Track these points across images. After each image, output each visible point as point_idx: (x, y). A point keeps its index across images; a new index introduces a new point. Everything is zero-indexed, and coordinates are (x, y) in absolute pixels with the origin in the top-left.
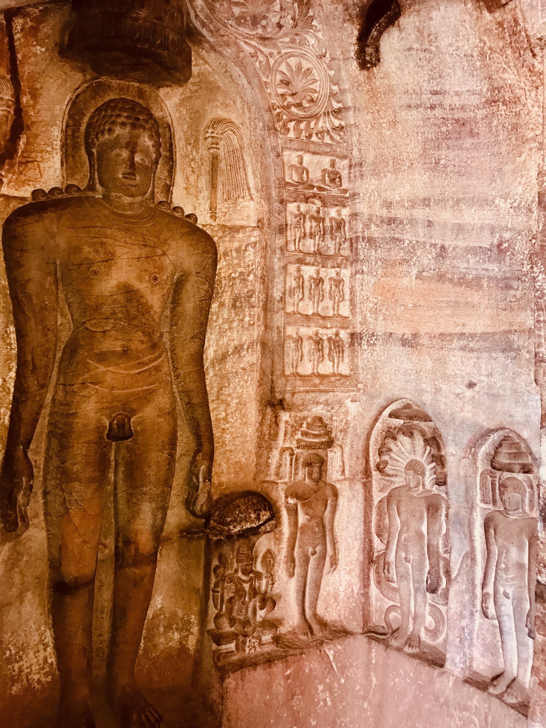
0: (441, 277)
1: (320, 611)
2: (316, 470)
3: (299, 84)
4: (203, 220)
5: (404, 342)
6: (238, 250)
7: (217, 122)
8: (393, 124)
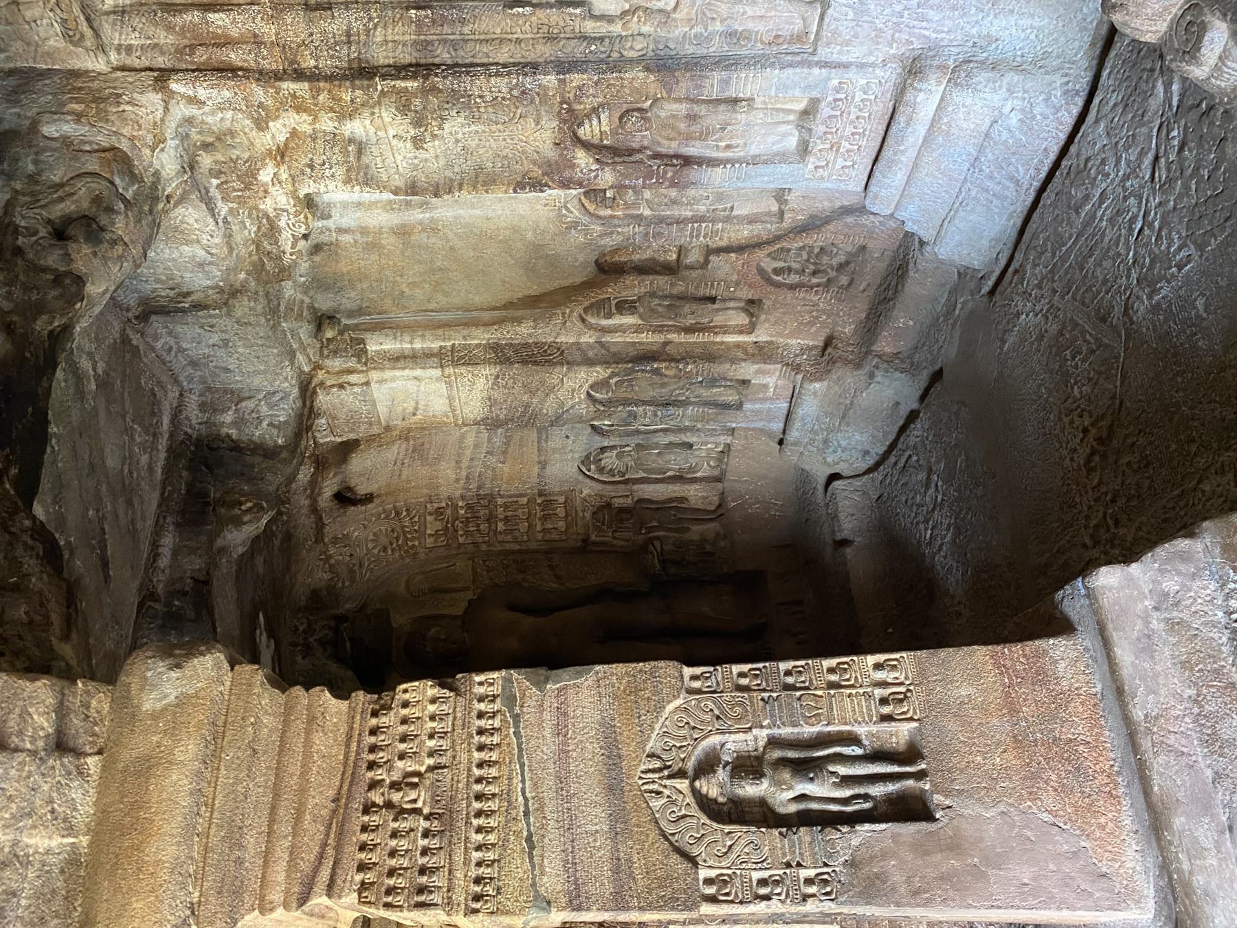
0: (505, 453)
1: (712, 508)
2: (624, 516)
3: (384, 540)
4: (470, 595)
5: (544, 468)
6: (488, 572)
7: (408, 588)
8: (409, 481)
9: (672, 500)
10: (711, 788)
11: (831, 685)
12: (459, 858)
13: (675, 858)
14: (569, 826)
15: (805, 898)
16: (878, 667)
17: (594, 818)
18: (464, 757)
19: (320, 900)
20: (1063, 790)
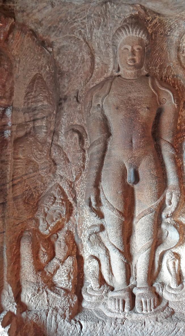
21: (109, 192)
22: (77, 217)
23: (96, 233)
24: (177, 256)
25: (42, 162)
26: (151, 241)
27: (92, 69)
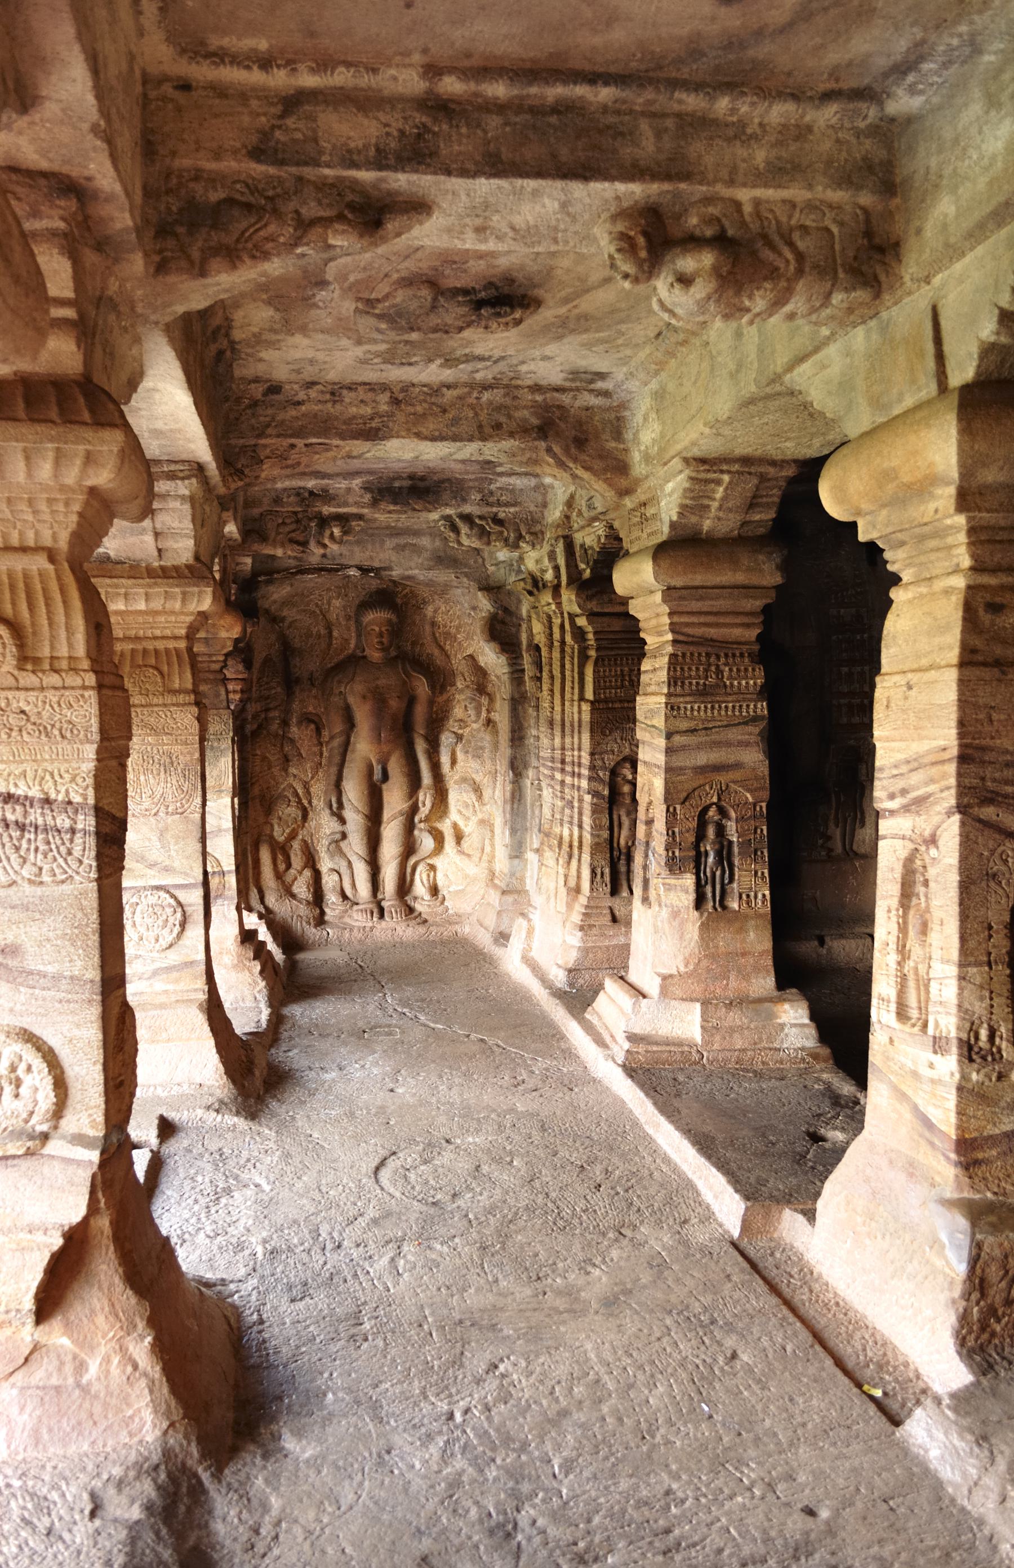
1: (855, 848)
9: (863, 813)
10: (712, 812)
11: (756, 873)
12: (688, 699)
13: (685, 794)
14: (699, 747)
15: (667, 850)
16: (764, 896)
17: (702, 759)
18: (730, 698)
19: (669, 637)
20: (709, 970)
21: (353, 791)
22: (313, 824)
23: (337, 842)
24: (433, 868)
25: (274, 757)
26: (401, 849)
27: (330, 644)
